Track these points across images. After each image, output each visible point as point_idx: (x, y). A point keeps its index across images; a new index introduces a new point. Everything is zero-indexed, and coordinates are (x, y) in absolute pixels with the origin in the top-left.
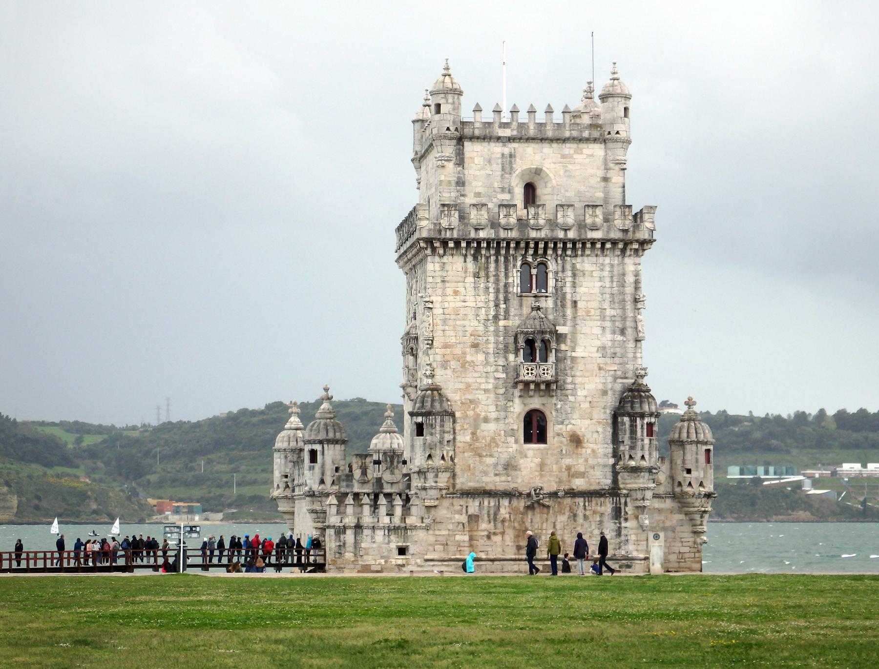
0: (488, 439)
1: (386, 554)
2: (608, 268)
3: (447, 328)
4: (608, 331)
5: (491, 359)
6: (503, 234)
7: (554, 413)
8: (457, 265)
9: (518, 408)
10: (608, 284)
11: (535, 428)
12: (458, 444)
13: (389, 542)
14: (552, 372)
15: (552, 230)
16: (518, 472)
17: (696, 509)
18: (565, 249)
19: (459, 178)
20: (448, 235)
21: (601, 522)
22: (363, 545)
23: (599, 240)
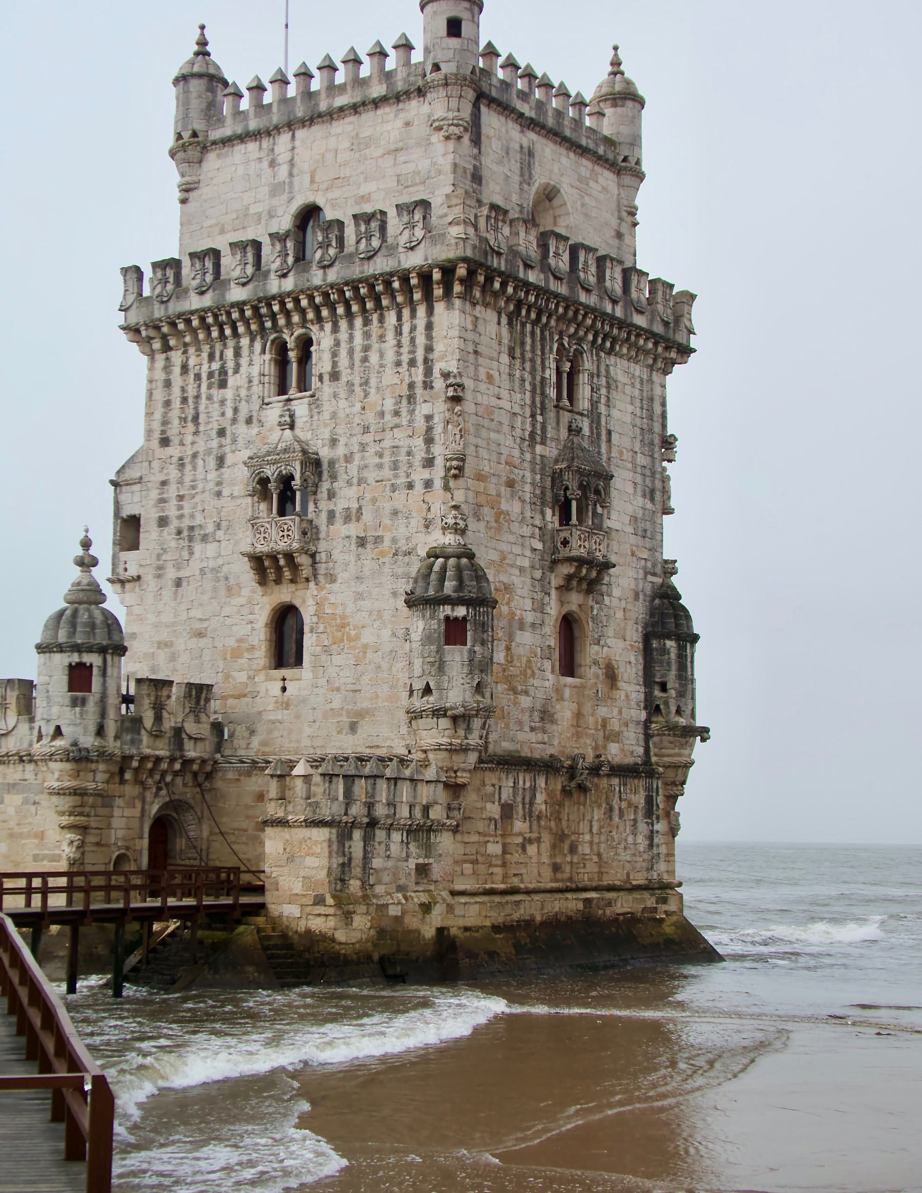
0: (524, 660)
1: (402, 881)
2: (638, 385)
3: (479, 442)
5: (528, 514)
6: (554, 286)
7: (590, 623)
8: (492, 327)
13: (408, 856)
15: (601, 298)
16: (555, 727)
19: (475, 166)
22: (377, 863)
23: (646, 331)
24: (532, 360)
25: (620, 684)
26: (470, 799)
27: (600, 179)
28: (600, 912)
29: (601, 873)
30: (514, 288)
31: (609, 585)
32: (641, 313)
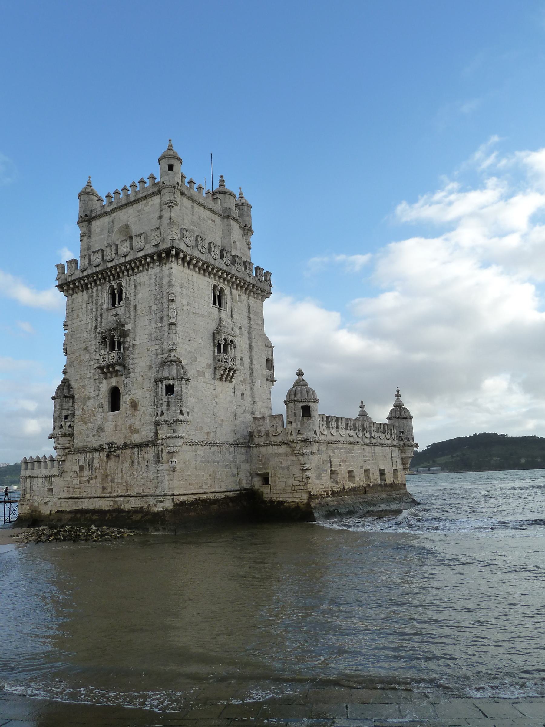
2: (153, 277)
4: (153, 322)
5: (93, 356)
7: (123, 387)
9: (105, 386)
10: (153, 288)
11: (115, 400)
12: (76, 417)
14: (115, 358)
17: (297, 452)
18: (128, 271)
20: (70, 279)
21: (147, 466)
23: (141, 257)
24: (97, 300)
25: (139, 408)
26: (67, 465)
27: (150, 203)
28: (122, 507)
29: (127, 490)
30: (79, 282)
31: (134, 368)
32: (142, 250)
